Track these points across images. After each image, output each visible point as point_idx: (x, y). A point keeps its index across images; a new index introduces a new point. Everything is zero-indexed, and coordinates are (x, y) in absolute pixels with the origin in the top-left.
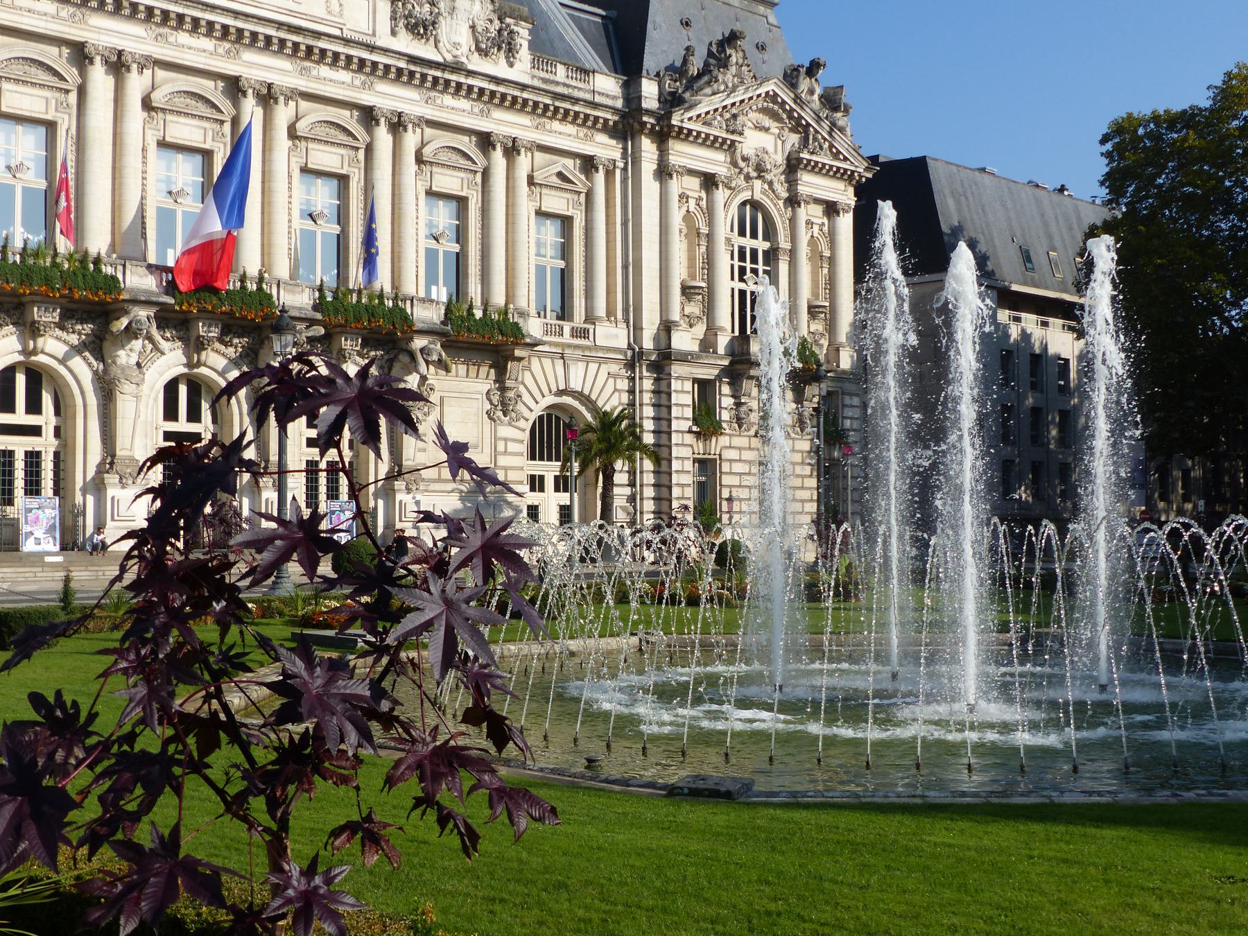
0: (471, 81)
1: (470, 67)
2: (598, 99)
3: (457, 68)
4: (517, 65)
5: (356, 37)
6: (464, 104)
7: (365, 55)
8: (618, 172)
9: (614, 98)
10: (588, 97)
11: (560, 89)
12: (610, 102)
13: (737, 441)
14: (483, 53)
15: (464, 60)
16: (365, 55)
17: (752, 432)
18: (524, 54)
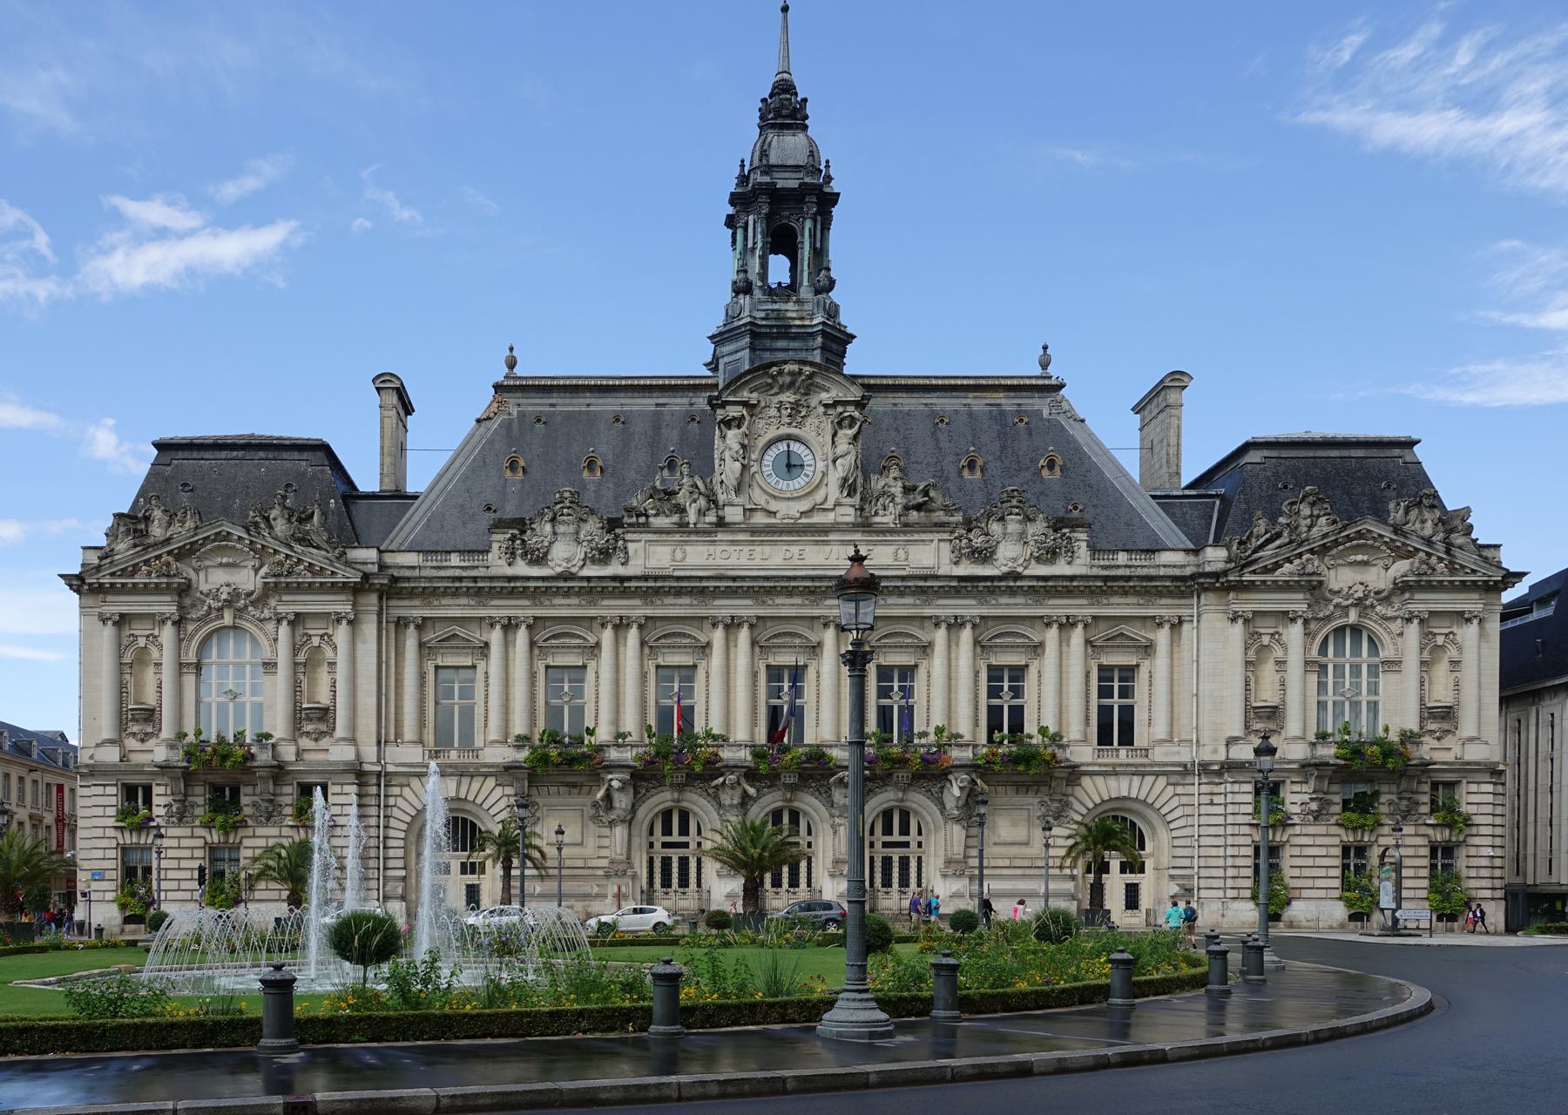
0: (1019, 583)
1: (1027, 572)
2: (1162, 572)
3: (1014, 576)
4: (1078, 561)
5: (922, 572)
6: (1020, 600)
7: (921, 583)
8: (1186, 627)
9: (1182, 566)
10: (1153, 572)
11: (1120, 572)
12: (1177, 572)
13: (1311, 830)
14: (1038, 560)
15: (1020, 569)
16: (921, 583)
17: (1333, 821)
18: (1083, 550)
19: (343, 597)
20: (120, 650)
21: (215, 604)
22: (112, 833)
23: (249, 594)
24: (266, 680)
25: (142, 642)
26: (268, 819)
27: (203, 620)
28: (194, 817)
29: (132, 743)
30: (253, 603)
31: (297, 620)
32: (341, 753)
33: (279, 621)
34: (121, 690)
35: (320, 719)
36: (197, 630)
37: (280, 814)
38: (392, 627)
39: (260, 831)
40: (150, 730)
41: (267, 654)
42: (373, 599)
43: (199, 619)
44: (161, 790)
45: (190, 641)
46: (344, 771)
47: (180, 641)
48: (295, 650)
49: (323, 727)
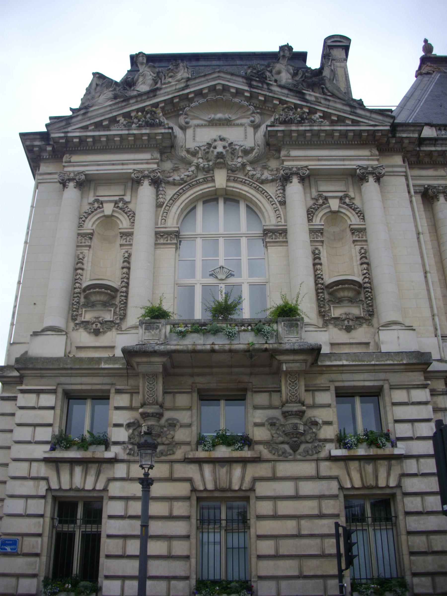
19: (365, 152)
20: (82, 219)
21: (202, 163)
22: (41, 470)
23: (246, 152)
24: (275, 252)
25: (108, 209)
26: (295, 448)
27: (186, 184)
28: (174, 445)
29: (83, 338)
30: (252, 163)
31: (308, 178)
32: (393, 342)
33: (286, 179)
34: (78, 265)
35: (351, 301)
36: (179, 194)
37: (315, 439)
38: (419, 197)
39: (284, 469)
40: (108, 317)
41: (271, 220)
42: (398, 160)
43: (183, 182)
44: (123, 400)
45: (170, 206)
46: (409, 367)
47: (159, 206)
48: (311, 213)
49: (356, 311)
